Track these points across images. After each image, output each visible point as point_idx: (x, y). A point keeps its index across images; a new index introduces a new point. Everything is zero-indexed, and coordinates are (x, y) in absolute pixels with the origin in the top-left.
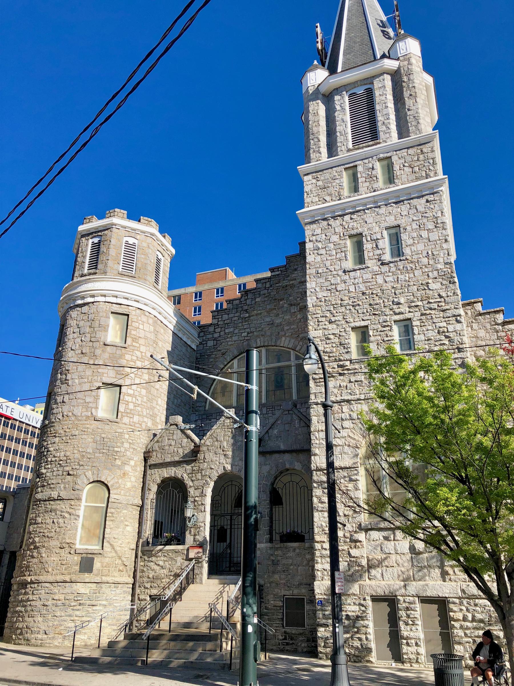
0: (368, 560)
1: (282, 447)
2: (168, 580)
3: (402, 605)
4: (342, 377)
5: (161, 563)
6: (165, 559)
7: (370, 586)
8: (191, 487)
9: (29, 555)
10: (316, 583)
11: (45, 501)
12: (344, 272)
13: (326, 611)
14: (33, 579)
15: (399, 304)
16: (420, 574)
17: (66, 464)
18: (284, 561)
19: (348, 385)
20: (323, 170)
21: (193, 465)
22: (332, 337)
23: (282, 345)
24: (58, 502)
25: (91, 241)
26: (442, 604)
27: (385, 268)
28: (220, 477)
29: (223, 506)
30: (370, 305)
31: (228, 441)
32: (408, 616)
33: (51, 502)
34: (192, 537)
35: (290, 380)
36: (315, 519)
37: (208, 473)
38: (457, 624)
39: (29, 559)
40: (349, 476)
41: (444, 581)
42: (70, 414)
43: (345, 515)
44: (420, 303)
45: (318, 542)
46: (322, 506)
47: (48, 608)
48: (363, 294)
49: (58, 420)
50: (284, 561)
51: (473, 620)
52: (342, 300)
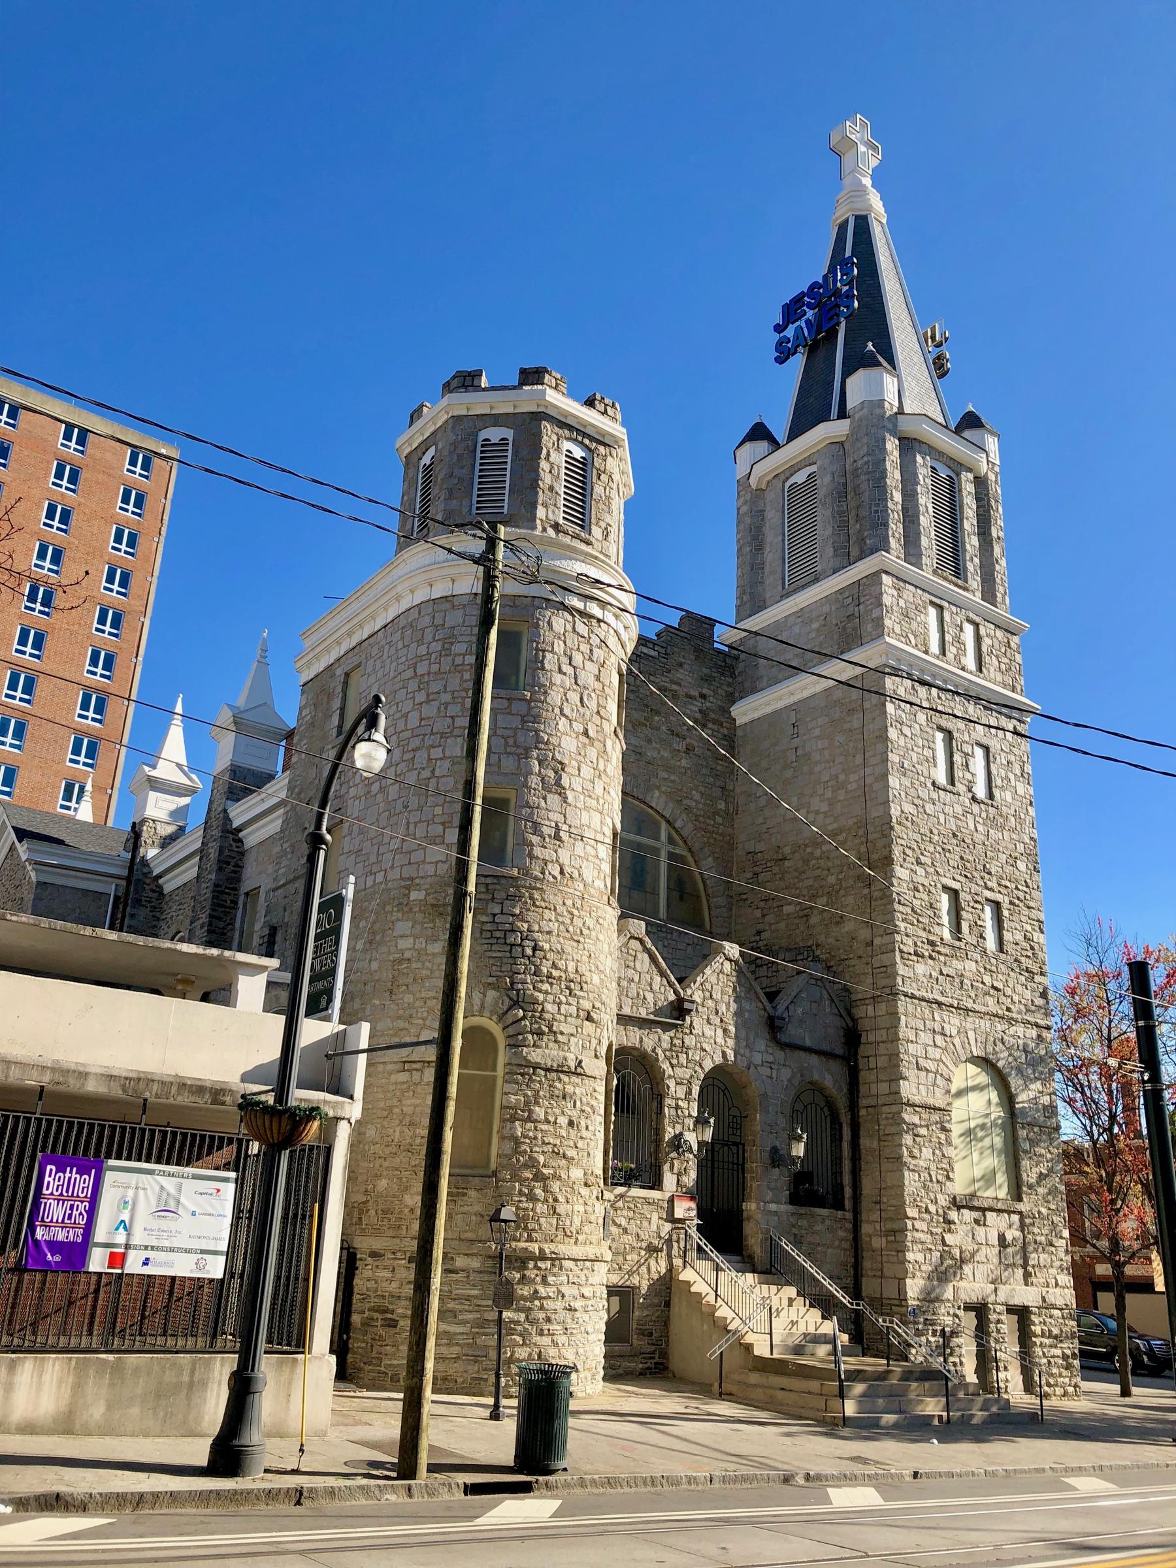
0: (961, 1252)
1: (808, 1043)
2: (636, 1258)
3: (993, 1317)
4: (931, 962)
5: (623, 1222)
6: (631, 1214)
7: (965, 1289)
8: (670, 1077)
9: (521, 1193)
10: (908, 1281)
11: (548, 1070)
12: (934, 784)
13: (918, 1323)
14: (547, 1251)
15: (989, 873)
16: (1006, 1273)
17: (582, 994)
18: (809, 1238)
19: (940, 977)
20: (905, 582)
21: (672, 1033)
22: (921, 888)
23: (654, 805)
24: (575, 1079)
25: (567, 445)
26: (1022, 1314)
27: (976, 808)
28: (716, 1069)
29: (726, 1124)
30: (962, 858)
31: (728, 1004)
32: (998, 1331)
33: (562, 1076)
34: (675, 1177)
35: (656, 880)
36: (907, 1183)
37: (697, 1058)
38: (1037, 1340)
39: (520, 1201)
40: (941, 1123)
41: (1026, 1285)
42: (576, 875)
43: (938, 1182)
44: (1008, 884)
45: (908, 1218)
46: (913, 1162)
47: (578, 1314)
48: (954, 835)
49: (551, 879)
50: (809, 1238)
51: (1050, 1336)
52: (931, 832)
